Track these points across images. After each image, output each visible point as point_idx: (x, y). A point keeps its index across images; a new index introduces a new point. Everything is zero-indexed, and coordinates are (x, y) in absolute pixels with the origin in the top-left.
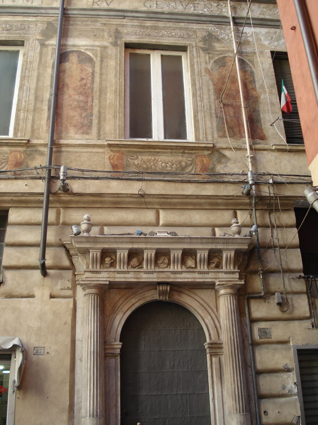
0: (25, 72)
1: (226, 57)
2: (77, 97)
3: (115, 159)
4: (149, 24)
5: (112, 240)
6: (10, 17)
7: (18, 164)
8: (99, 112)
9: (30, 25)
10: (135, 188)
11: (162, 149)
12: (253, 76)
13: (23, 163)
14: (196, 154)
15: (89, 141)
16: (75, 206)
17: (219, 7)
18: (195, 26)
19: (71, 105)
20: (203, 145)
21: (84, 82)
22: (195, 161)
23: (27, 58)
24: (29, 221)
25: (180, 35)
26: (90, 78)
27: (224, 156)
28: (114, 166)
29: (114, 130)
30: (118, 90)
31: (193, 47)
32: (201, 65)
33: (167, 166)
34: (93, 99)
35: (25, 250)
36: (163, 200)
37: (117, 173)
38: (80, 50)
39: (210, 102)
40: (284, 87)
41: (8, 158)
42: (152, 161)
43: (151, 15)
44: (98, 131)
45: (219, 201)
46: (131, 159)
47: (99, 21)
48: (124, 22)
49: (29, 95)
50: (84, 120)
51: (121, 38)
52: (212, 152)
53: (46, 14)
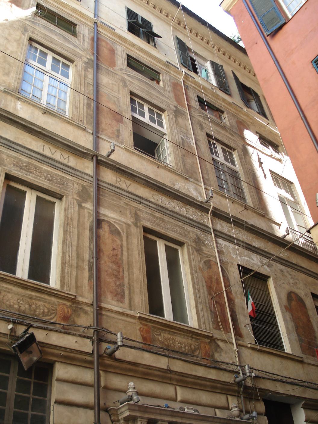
0: (67, 228)
1: (211, 260)
2: (111, 265)
3: (144, 331)
4: (157, 215)
5: (158, 411)
6: (51, 168)
7: (66, 318)
8: (129, 283)
9: (68, 183)
10: (162, 363)
11: (177, 330)
12: (229, 281)
13: (70, 318)
14: (201, 340)
15: (124, 309)
16: (112, 370)
17: (202, 216)
18: (189, 228)
19: (107, 271)
20: (206, 334)
21: (115, 252)
22: (201, 347)
23: (68, 214)
24: (76, 380)
25: (180, 233)
26: (120, 250)
27: (218, 346)
28: (144, 339)
29: (142, 304)
30: (141, 267)
31: (189, 245)
32: (195, 263)
33: (182, 347)
34: (123, 271)
35: (75, 409)
36: (181, 378)
37: (148, 346)
38: (109, 221)
39: (205, 296)
40: (250, 296)
41: (57, 309)
42: (171, 339)
43: (159, 208)
44: (129, 301)
45: (219, 385)
46: (156, 334)
47: (122, 200)
48: (140, 207)
49: (72, 251)
50: (118, 288)
51: (140, 221)
52: (211, 341)
53: (81, 177)
